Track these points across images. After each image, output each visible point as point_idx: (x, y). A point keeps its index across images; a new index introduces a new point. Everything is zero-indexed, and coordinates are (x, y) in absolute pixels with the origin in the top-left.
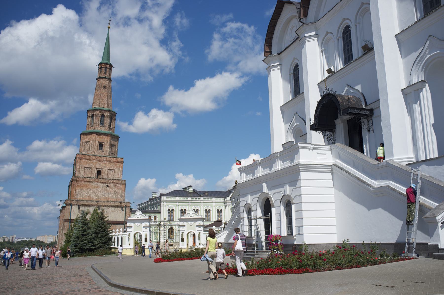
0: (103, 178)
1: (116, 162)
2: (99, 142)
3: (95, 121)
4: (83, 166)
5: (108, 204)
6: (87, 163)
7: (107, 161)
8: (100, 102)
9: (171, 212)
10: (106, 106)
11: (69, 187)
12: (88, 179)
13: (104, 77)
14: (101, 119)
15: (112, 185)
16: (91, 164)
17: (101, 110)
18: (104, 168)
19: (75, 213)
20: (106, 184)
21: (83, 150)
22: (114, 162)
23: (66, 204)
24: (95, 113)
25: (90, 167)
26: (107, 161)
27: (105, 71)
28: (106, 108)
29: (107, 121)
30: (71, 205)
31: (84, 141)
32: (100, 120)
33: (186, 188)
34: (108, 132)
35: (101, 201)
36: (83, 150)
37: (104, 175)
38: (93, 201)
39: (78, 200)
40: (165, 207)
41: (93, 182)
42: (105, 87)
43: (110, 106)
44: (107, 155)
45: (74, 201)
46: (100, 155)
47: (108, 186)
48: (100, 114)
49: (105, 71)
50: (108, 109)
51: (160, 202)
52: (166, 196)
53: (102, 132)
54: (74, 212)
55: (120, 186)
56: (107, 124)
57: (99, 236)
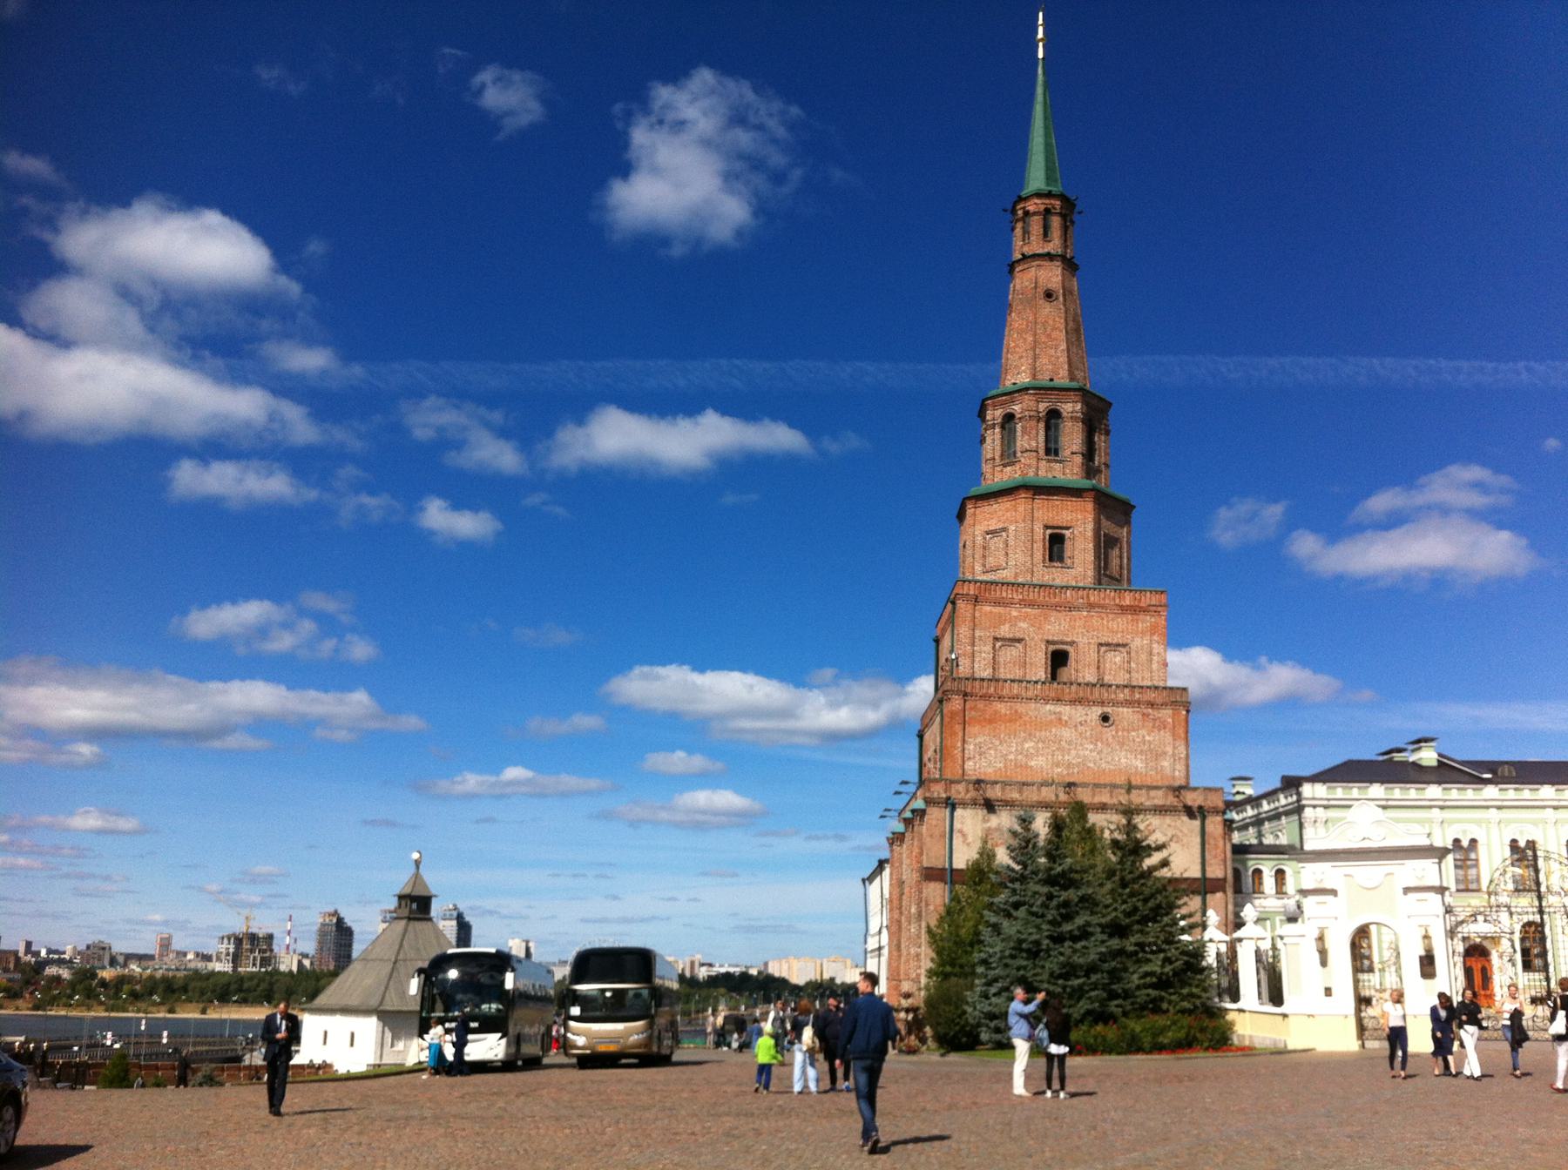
1: (1134, 610)
2: (1047, 527)
3: (1022, 442)
4: (990, 633)
6: (1001, 620)
7: (1091, 606)
8: (1035, 358)
10: (1063, 372)
11: (921, 736)
12: (1016, 688)
13: (1040, 251)
14: (1048, 428)
16: (1023, 625)
17: (1041, 390)
19: (971, 837)
20: (1098, 711)
21: (978, 568)
22: (1124, 610)
23: (929, 801)
25: (1018, 635)
28: (1062, 379)
29: (1072, 438)
30: (951, 805)
32: (1042, 433)
35: (1084, 785)
37: (1082, 669)
39: (978, 782)
41: (1036, 699)
42: (1049, 295)
44: (1089, 580)
45: (961, 787)
46: (1058, 582)
47: (1105, 718)
48: (1042, 407)
50: (1074, 385)
51: (1298, 809)
54: (964, 835)
55: (1166, 714)
56: (1075, 448)
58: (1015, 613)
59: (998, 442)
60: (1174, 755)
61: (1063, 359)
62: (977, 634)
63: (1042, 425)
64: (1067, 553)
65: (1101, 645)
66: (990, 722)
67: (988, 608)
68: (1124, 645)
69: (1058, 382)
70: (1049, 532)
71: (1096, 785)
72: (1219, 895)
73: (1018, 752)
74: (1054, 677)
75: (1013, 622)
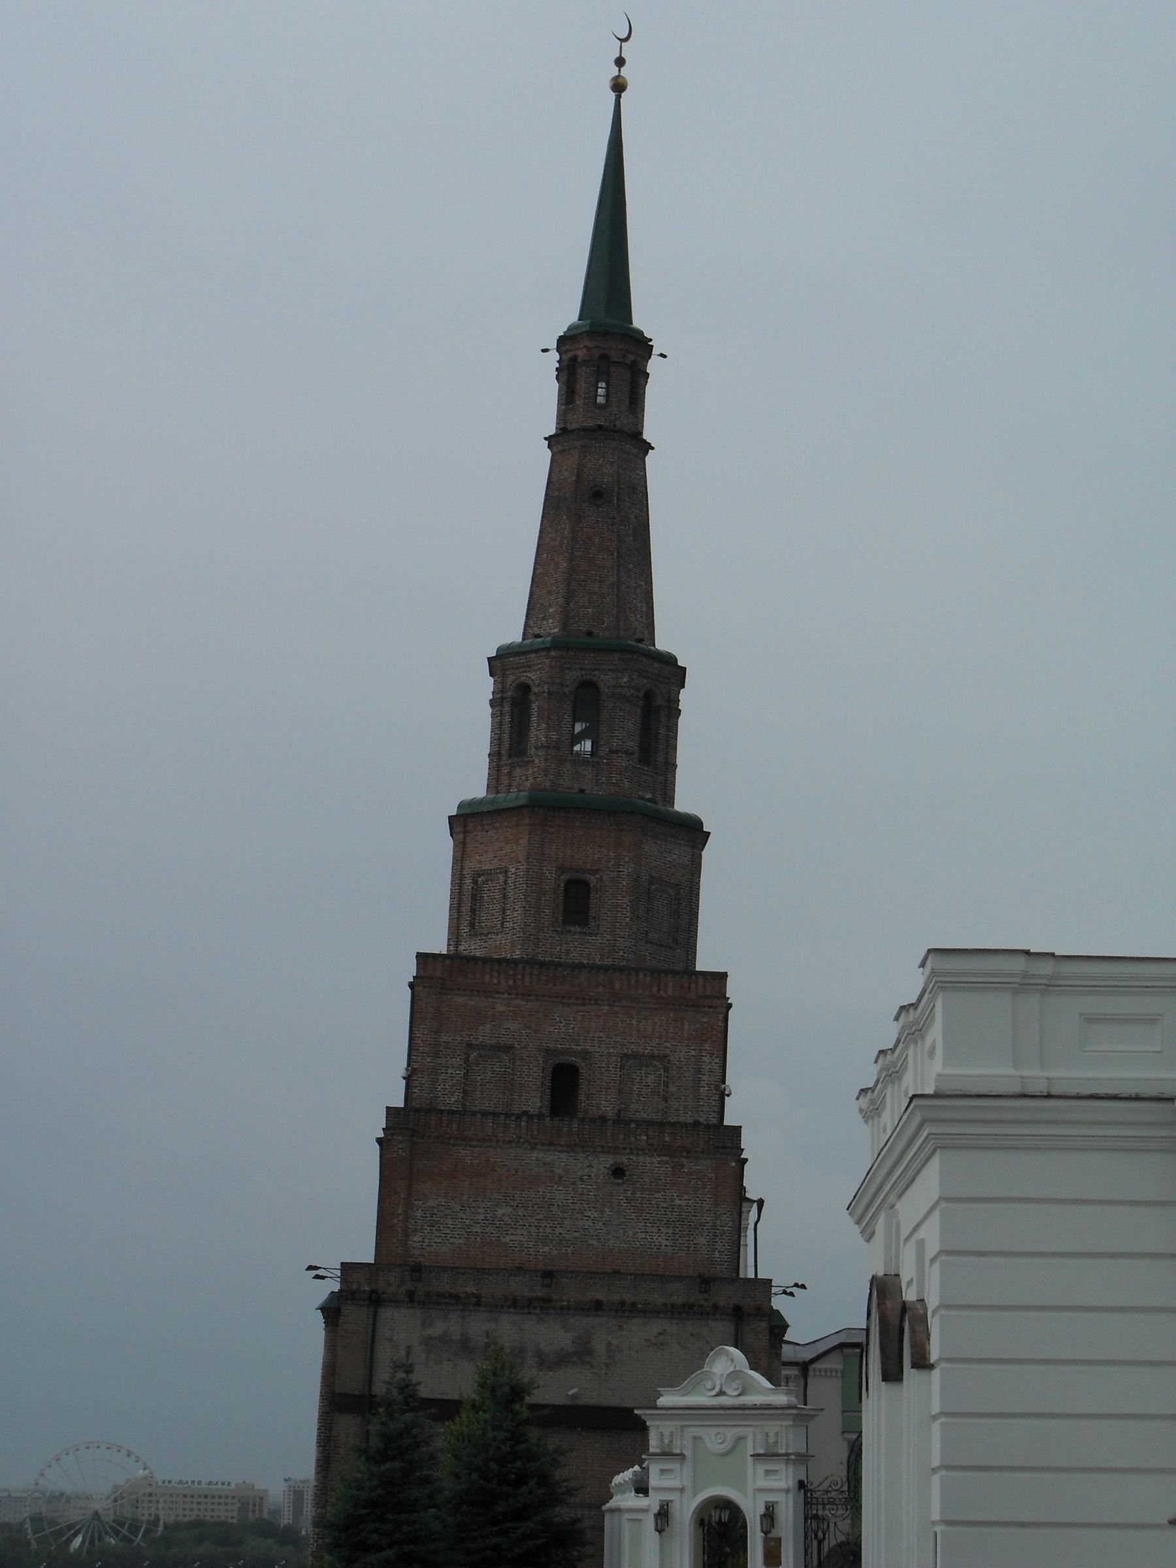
2: (561, 869)
3: (538, 733)
8: (570, 595)
13: (590, 424)
15: (652, 1165)
16: (513, 1026)
30: (375, 1300)
31: (471, 865)
37: (599, 1098)
39: (417, 1270)
42: (597, 495)
47: (618, 1172)
58: (501, 1008)
59: (506, 727)
64: (592, 913)
65: (625, 1056)
67: (460, 1000)
70: (565, 877)
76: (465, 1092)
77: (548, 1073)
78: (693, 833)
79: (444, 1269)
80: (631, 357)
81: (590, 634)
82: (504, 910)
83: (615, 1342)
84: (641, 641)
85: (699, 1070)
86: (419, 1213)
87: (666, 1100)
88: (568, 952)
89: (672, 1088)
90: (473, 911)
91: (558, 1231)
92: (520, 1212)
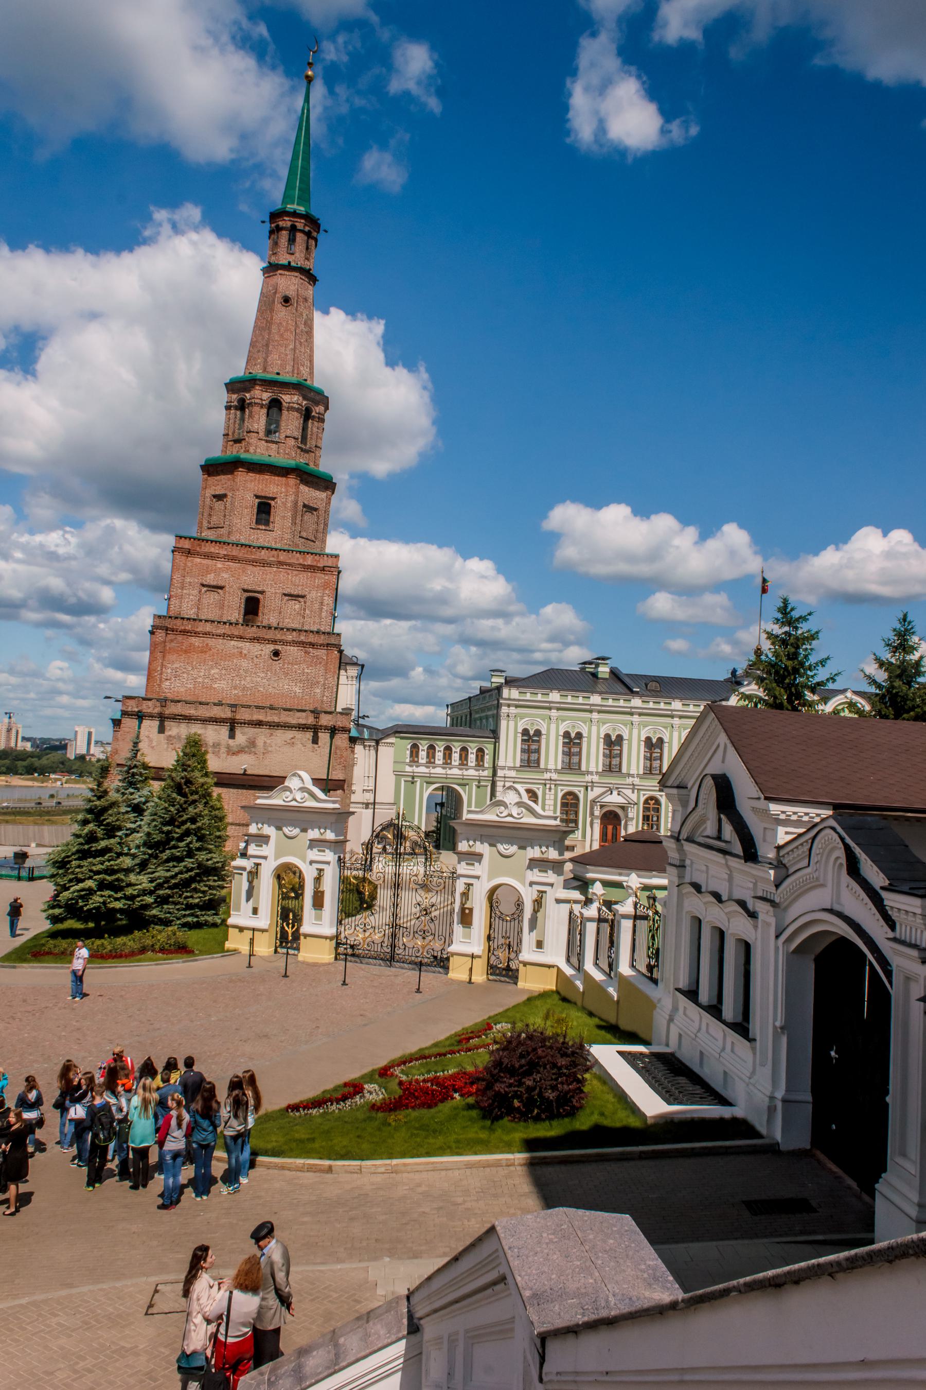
0: (265, 623)
2: (257, 497)
5: (269, 719)
7: (281, 563)
9: (531, 739)
10: (289, 368)
12: (208, 627)
13: (285, 262)
16: (225, 575)
18: (270, 591)
20: (272, 647)
21: (205, 524)
23: (124, 713)
24: (248, 395)
25: (220, 583)
26: (281, 563)
27: (292, 241)
28: (285, 377)
30: (140, 716)
33: (590, 663)
34: (291, 463)
36: (205, 524)
37: (268, 616)
38: (220, 704)
39: (164, 702)
40: (512, 723)
41: (223, 636)
42: (286, 300)
43: (304, 371)
45: (150, 703)
46: (261, 542)
47: (276, 653)
48: (266, 396)
49: (292, 241)
50: (294, 379)
51: (498, 706)
52: (518, 687)
53: (266, 459)
54: (151, 741)
55: (322, 653)
56: (289, 433)
57: (164, 856)
60: (324, 684)
61: (290, 357)
62: (188, 580)
63: (265, 411)
64: (271, 519)
65: (285, 595)
66: (186, 652)
67: (199, 560)
68: (303, 597)
69: (280, 378)
70: (257, 501)
71: (257, 707)
72: (339, 792)
73: (205, 677)
74: (244, 620)
75: (217, 572)
76: (198, 609)
77: (243, 601)
78: (326, 484)
79: (179, 701)
80: (307, 229)
81: (278, 374)
82: (225, 516)
83: (268, 741)
84: (306, 380)
85: (322, 603)
86: (169, 671)
87: (304, 617)
88: (258, 539)
89: (307, 612)
90: (210, 515)
91: (243, 683)
92: (224, 672)
